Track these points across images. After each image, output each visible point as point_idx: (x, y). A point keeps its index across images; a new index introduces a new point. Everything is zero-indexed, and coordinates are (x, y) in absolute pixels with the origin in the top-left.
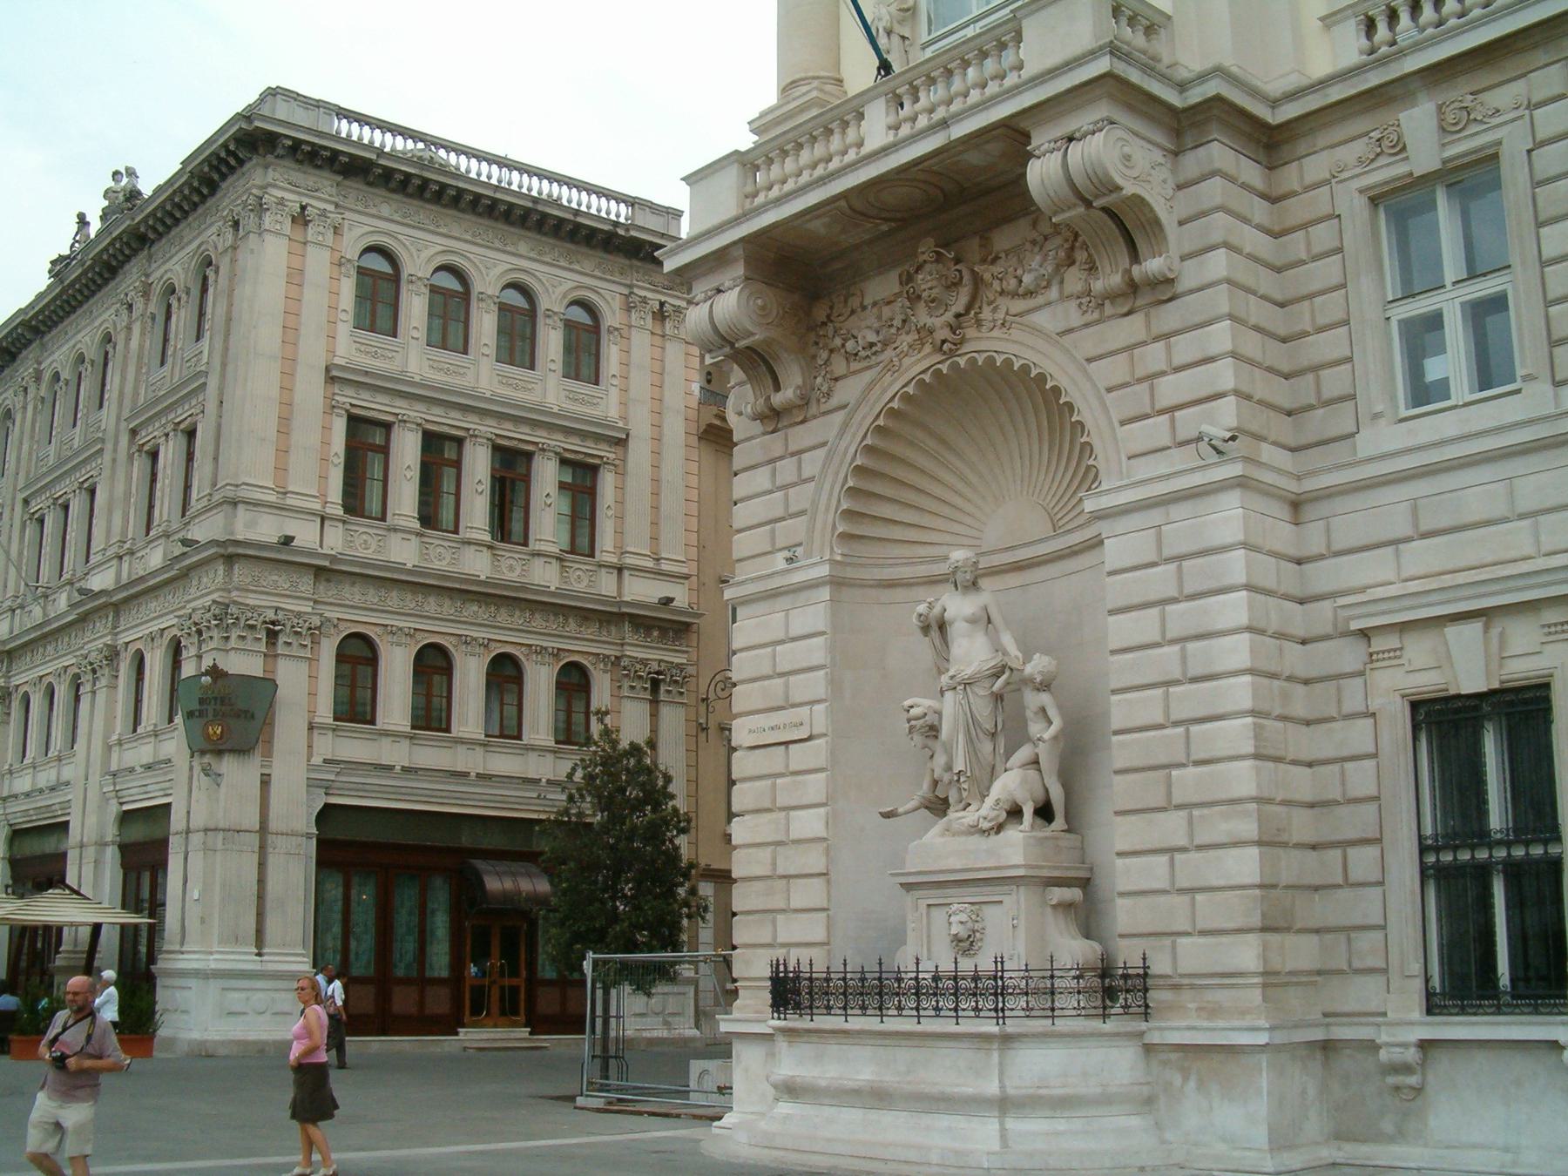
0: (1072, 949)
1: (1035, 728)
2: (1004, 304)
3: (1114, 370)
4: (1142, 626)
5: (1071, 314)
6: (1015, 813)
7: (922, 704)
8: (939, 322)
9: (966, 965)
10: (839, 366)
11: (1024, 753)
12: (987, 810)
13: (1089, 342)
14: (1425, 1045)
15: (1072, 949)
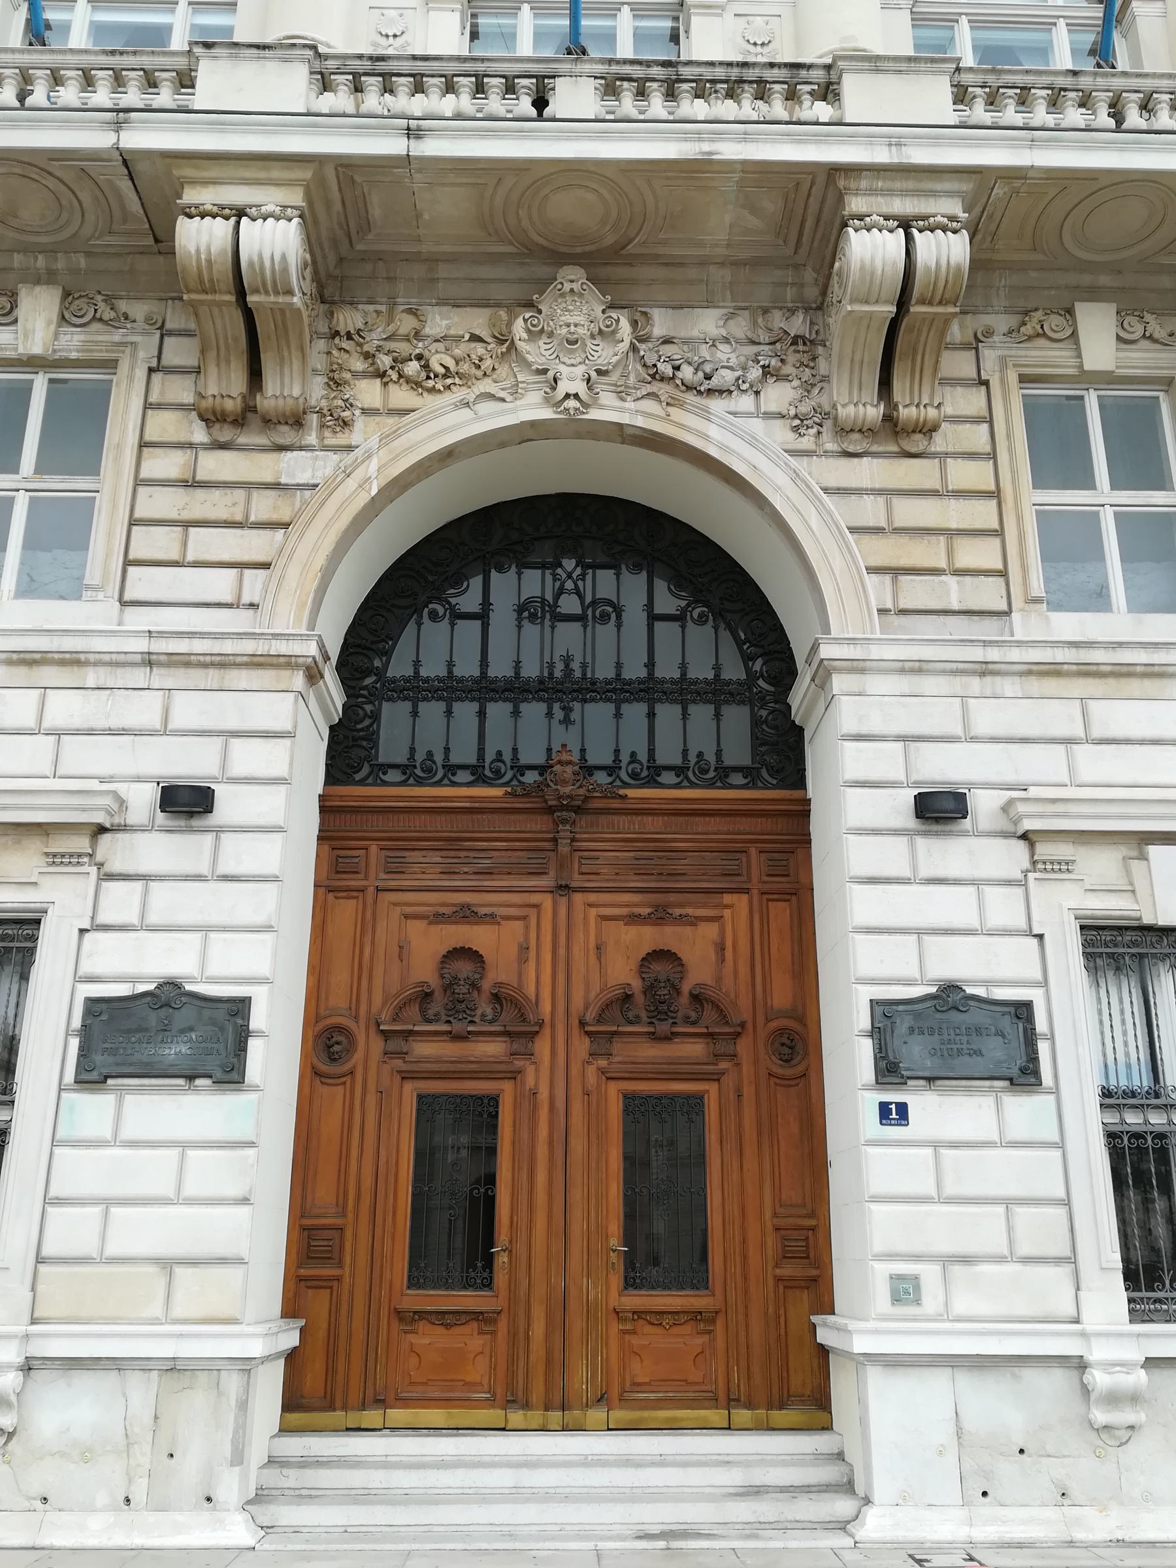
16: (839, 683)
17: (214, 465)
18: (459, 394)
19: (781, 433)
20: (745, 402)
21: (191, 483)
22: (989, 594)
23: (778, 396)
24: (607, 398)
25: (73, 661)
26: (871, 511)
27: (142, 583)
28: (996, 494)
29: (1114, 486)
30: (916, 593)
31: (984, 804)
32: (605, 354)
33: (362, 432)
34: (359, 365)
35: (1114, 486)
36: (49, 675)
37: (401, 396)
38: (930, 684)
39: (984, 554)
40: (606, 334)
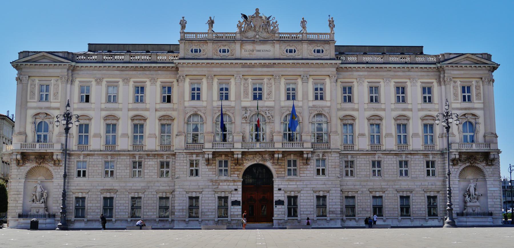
0: (47, 213)
1: (44, 196)
2: (46, 162)
3: (56, 170)
4: (57, 190)
5: (52, 165)
6: (43, 202)
7: (34, 193)
8: (39, 162)
9: (37, 214)
10: (27, 162)
11: (43, 198)
12: (41, 202)
13: (54, 167)
14: (75, 220)
15: (47, 213)
16: (274, 181)
17: (235, 167)
18: (251, 161)
19: (271, 164)
20: (269, 162)
21: (234, 168)
22: (284, 175)
23: (271, 161)
24: (260, 161)
25: (228, 181)
26: (277, 170)
27: (232, 175)
28: (285, 168)
29: (293, 167)
30: (279, 175)
31: (282, 189)
32: (260, 159)
33: (245, 164)
34: (244, 159)
35: (293, 167)
36: (227, 182)
37: (247, 162)
38: (280, 181)
39: (283, 172)
40: (260, 157)
